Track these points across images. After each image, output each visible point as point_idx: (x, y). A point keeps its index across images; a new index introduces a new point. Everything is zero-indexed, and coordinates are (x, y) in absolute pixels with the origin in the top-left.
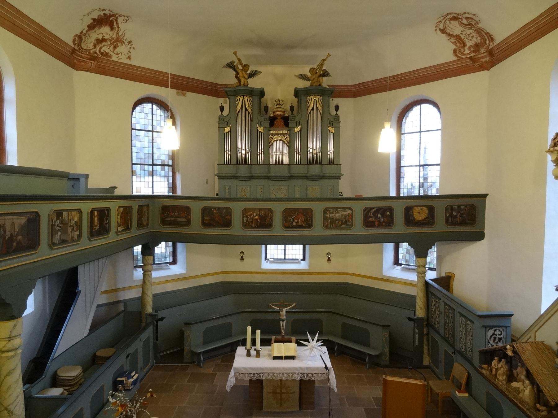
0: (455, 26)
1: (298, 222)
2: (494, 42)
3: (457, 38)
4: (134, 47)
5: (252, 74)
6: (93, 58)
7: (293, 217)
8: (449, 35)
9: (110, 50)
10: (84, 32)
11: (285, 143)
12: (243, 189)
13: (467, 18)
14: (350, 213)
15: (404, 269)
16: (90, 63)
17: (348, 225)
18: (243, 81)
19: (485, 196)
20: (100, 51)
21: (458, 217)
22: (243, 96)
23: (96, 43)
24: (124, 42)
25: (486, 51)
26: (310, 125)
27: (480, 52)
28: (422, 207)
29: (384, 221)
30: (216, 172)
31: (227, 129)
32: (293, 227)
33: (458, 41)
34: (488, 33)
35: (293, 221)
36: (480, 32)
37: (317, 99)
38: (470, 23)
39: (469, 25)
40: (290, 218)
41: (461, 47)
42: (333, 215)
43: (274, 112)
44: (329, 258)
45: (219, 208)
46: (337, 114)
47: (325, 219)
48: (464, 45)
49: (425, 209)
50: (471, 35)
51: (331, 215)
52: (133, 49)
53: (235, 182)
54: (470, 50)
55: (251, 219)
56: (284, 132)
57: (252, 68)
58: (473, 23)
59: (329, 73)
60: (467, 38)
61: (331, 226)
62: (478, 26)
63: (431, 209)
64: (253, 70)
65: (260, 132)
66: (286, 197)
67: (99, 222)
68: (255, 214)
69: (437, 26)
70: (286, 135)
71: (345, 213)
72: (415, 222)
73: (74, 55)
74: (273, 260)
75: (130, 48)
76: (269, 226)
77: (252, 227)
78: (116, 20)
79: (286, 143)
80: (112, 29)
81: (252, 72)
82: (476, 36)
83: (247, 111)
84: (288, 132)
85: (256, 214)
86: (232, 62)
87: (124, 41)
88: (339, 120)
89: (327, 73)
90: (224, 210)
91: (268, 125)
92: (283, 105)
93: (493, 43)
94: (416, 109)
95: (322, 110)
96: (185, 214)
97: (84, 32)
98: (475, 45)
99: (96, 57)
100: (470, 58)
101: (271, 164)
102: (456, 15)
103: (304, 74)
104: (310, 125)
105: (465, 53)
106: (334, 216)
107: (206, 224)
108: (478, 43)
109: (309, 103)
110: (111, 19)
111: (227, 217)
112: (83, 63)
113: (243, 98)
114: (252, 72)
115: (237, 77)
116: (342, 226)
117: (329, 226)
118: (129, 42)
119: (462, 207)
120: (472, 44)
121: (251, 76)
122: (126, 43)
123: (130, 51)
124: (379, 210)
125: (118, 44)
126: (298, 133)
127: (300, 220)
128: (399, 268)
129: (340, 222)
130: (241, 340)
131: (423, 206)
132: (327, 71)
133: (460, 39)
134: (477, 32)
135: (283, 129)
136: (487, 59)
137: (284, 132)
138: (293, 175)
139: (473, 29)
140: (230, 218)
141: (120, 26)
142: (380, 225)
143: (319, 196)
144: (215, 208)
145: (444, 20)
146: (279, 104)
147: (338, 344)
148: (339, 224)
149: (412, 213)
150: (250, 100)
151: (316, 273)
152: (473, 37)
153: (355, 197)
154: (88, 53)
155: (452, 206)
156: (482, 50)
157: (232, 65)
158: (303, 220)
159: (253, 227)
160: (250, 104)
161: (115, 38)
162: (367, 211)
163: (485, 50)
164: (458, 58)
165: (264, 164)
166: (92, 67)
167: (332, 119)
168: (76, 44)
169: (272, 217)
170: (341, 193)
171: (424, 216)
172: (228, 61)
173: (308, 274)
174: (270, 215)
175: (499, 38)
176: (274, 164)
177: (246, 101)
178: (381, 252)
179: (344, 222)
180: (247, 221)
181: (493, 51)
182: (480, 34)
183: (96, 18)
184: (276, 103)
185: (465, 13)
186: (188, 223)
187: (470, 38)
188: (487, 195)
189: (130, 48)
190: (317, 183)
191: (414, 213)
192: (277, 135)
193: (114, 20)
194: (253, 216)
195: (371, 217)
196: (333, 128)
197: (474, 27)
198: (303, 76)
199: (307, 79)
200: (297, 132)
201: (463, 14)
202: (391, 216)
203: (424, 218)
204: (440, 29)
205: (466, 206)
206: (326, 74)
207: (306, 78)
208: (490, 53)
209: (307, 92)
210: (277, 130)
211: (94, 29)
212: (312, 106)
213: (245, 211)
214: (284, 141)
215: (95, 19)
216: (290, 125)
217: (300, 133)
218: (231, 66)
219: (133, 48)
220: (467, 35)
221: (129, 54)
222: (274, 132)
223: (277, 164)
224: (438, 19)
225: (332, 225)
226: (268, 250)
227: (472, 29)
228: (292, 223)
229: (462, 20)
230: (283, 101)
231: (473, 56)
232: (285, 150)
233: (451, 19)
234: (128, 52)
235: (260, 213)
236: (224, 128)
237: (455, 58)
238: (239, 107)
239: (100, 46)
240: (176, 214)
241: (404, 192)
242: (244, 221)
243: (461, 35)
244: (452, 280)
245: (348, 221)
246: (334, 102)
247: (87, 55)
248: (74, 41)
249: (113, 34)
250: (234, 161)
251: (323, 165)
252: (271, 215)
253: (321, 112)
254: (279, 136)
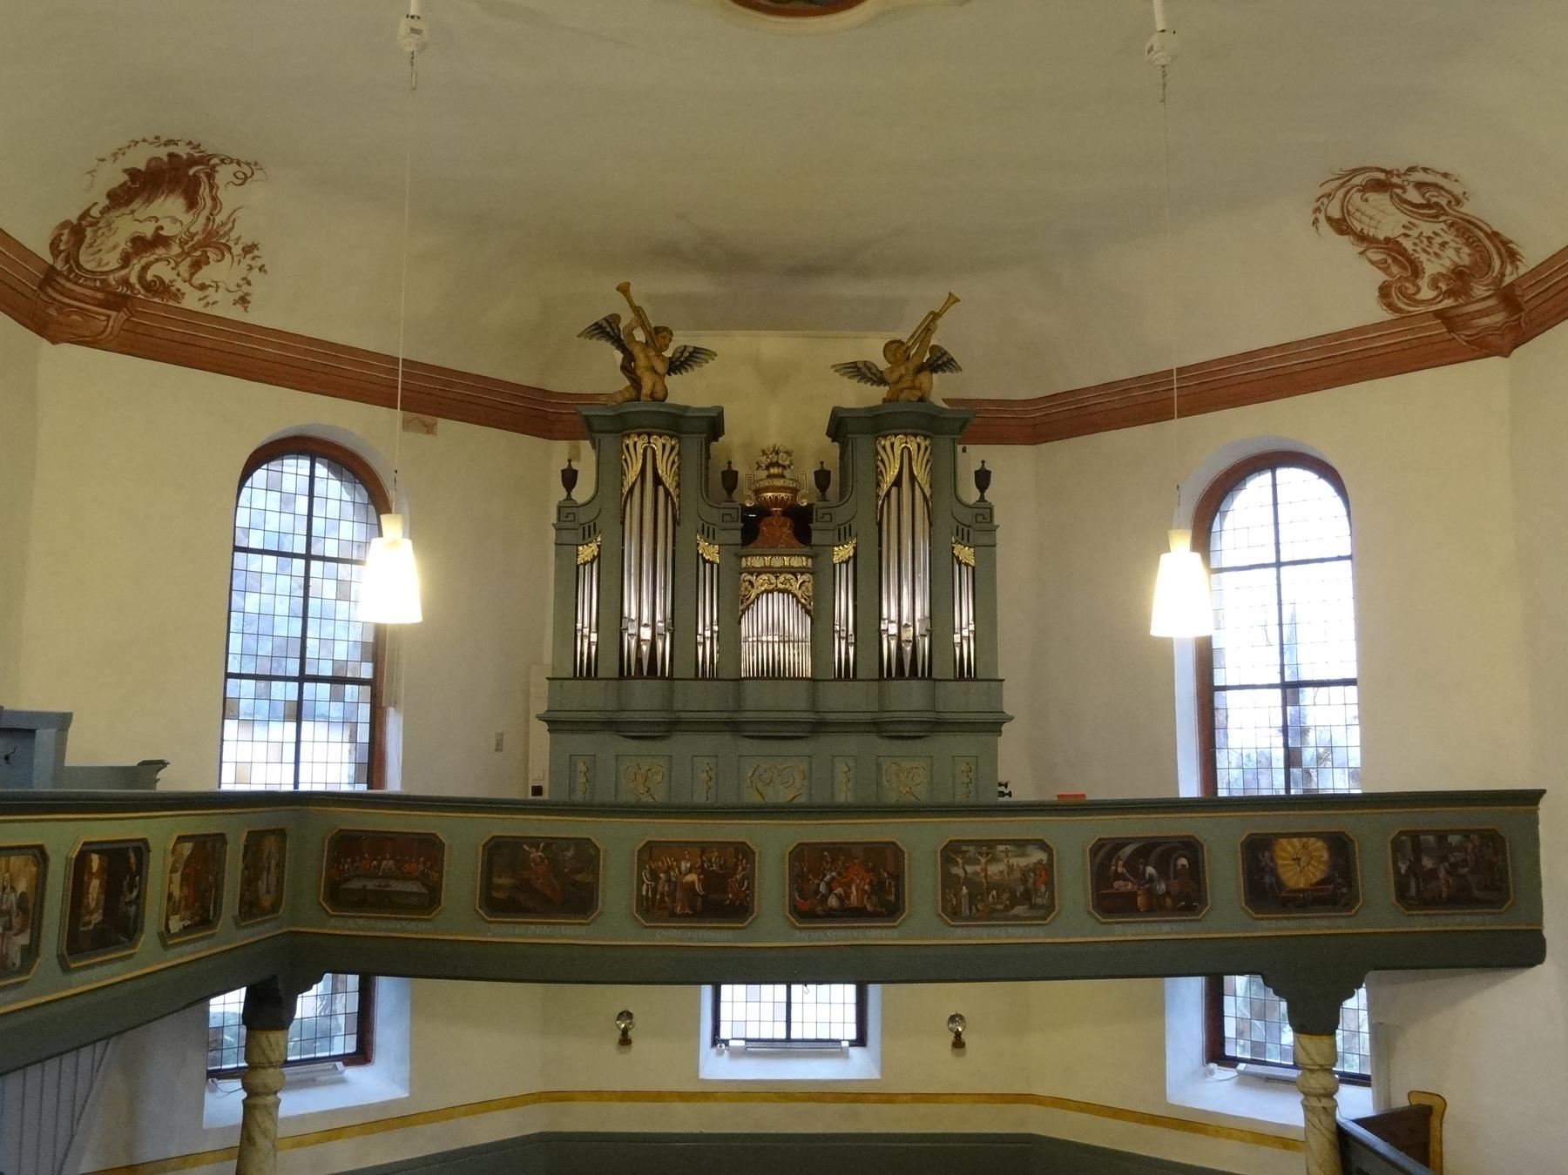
0: (1380, 208)
1: (848, 895)
2: (1518, 263)
3: (1391, 250)
4: (263, 266)
5: (682, 359)
6: (116, 300)
7: (828, 877)
8: (1362, 238)
9: (178, 275)
10: (95, 212)
11: (798, 602)
12: (643, 771)
13: (1419, 185)
14: (1040, 862)
15: (1246, 1080)
16: (104, 318)
17: (1033, 907)
18: (647, 383)
19: (1533, 797)
20: (141, 278)
21: (1442, 874)
22: (649, 435)
23: (130, 250)
24: (229, 249)
25: (1490, 293)
26: (888, 540)
27: (1474, 295)
28: (1305, 840)
29: (1168, 893)
30: (542, 708)
31: (587, 552)
32: (830, 915)
33: (1395, 260)
34: (1496, 234)
35: (830, 890)
36: (1469, 230)
37: (913, 447)
38: (1434, 200)
39: (1428, 206)
40: (816, 881)
41: (1406, 279)
42: (978, 868)
43: (758, 492)
44: (958, 1035)
45: (550, 843)
46: (982, 499)
47: (949, 882)
48: (1416, 271)
49: (1317, 845)
50: (1438, 240)
51: (969, 869)
52: (260, 269)
53: (609, 746)
54: (1437, 287)
55: (669, 886)
56: (797, 562)
57: (681, 340)
58: (1444, 202)
59: (952, 359)
60: (1424, 251)
61: (971, 909)
62: (1460, 212)
63: (1340, 845)
64: (685, 347)
65: (708, 561)
66: (803, 799)
67: (102, 897)
68: (685, 865)
69: (1317, 210)
70: (802, 574)
71: (1022, 862)
72: (1283, 894)
73: (50, 291)
74: (742, 1043)
75: (251, 268)
76: (888, 907)
77: (673, 915)
78: (210, 176)
79: (803, 601)
80: (192, 204)
81: (682, 353)
82: (1457, 243)
83: (661, 489)
84: (810, 560)
85: (689, 865)
86: (613, 320)
87: (231, 244)
88: (991, 521)
89: (945, 359)
90: (567, 850)
91: (737, 537)
92: (789, 466)
93: (1517, 268)
94: (1258, 485)
95: (931, 486)
96: (421, 867)
97: (95, 212)
98: (1453, 271)
99: (126, 297)
100: (1439, 314)
101: (746, 678)
102: (1382, 176)
103: (865, 363)
104: (888, 540)
105: (1420, 296)
106: (982, 874)
107: (496, 905)
108: (1464, 266)
109: (882, 461)
110: (191, 172)
111: (579, 877)
112: (78, 318)
113: (649, 443)
114: (682, 353)
115: (628, 368)
116: (1012, 912)
117: (965, 911)
118: (249, 246)
119: (1454, 839)
120: (1444, 271)
121: (677, 365)
122: (237, 250)
123: (249, 278)
124: (1148, 848)
125: (209, 254)
126: (844, 566)
127: (854, 889)
128: (1230, 1073)
129: (1005, 896)
131: (1309, 835)
132: (946, 353)
133: (1403, 252)
134: (1458, 230)
135: (788, 551)
136: (1498, 318)
137: (797, 562)
138: (830, 717)
139: (1445, 221)
140: (590, 878)
141: (221, 194)
142: (1155, 907)
143: (923, 795)
144: (534, 842)
145: (1343, 191)
146: (776, 464)
148: (1001, 903)
149: (1272, 860)
150: (673, 448)
151: (910, 1097)
152: (1443, 245)
153: (1056, 799)
154: (98, 284)
155: (1415, 836)
156: (1480, 290)
157: (613, 329)
158: (866, 887)
159: (679, 916)
160: (673, 462)
161: (200, 233)
162: (1104, 853)
163: (1487, 290)
164: (1398, 315)
165: (720, 676)
166: (109, 329)
167: (967, 517)
168: (61, 252)
169: (750, 877)
170: (1006, 786)
171: (1316, 872)
172: (599, 317)
173: (875, 1102)
174: (740, 868)
175: (1533, 254)
176: (758, 678)
177: (659, 453)
178: (1157, 1011)
179: (1018, 894)
180: (655, 891)
181: (1518, 292)
182: (1470, 237)
183: (142, 166)
184: (764, 461)
185: (1412, 169)
186: (430, 901)
187: (1436, 248)
188: (1541, 793)
189: (251, 268)
190: (918, 746)
191: (1280, 862)
192: (766, 573)
193: (202, 175)
194: (680, 872)
195: (1119, 877)
196: (972, 550)
197: (1446, 214)
198: (860, 369)
199: (879, 379)
200: (843, 562)
201: (1407, 170)
202: (1196, 870)
203: (1315, 881)
204: (1329, 219)
205: (1467, 837)
206: (941, 362)
207: (871, 373)
208: (1508, 298)
209: (877, 423)
210: (767, 555)
211: (128, 202)
212: (896, 471)
213: (650, 851)
214: (794, 596)
215: (139, 171)
216: (816, 537)
217: (851, 562)
218: (609, 333)
219: (261, 269)
220: (1425, 240)
221: (246, 288)
222: (757, 562)
223: (768, 678)
224: (1321, 186)
225: (973, 907)
226: (722, 1004)
227: (1440, 220)
228: (825, 898)
229: (1405, 191)
230: (788, 453)
231: (1452, 307)
232: (799, 626)
233: (1364, 189)
234: (241, 282)
235: (703, 862)
236: (577, 545)
237: (1387, 316)
238: (632, 475)
239: (144, 261)
240: (388, 864)
241: (1230, 783)
242: (644, 893)
243: (1401, 240)
244: (1434, 1121)
245: (1036, 890)
246: (973, 457)
247: (96, 289)
248: (54, 246)
249: (193, 222)
250: (609, 667)
251: (936, 680)
252: (744, 869)
253: (928, 494)
254: (777, 577)
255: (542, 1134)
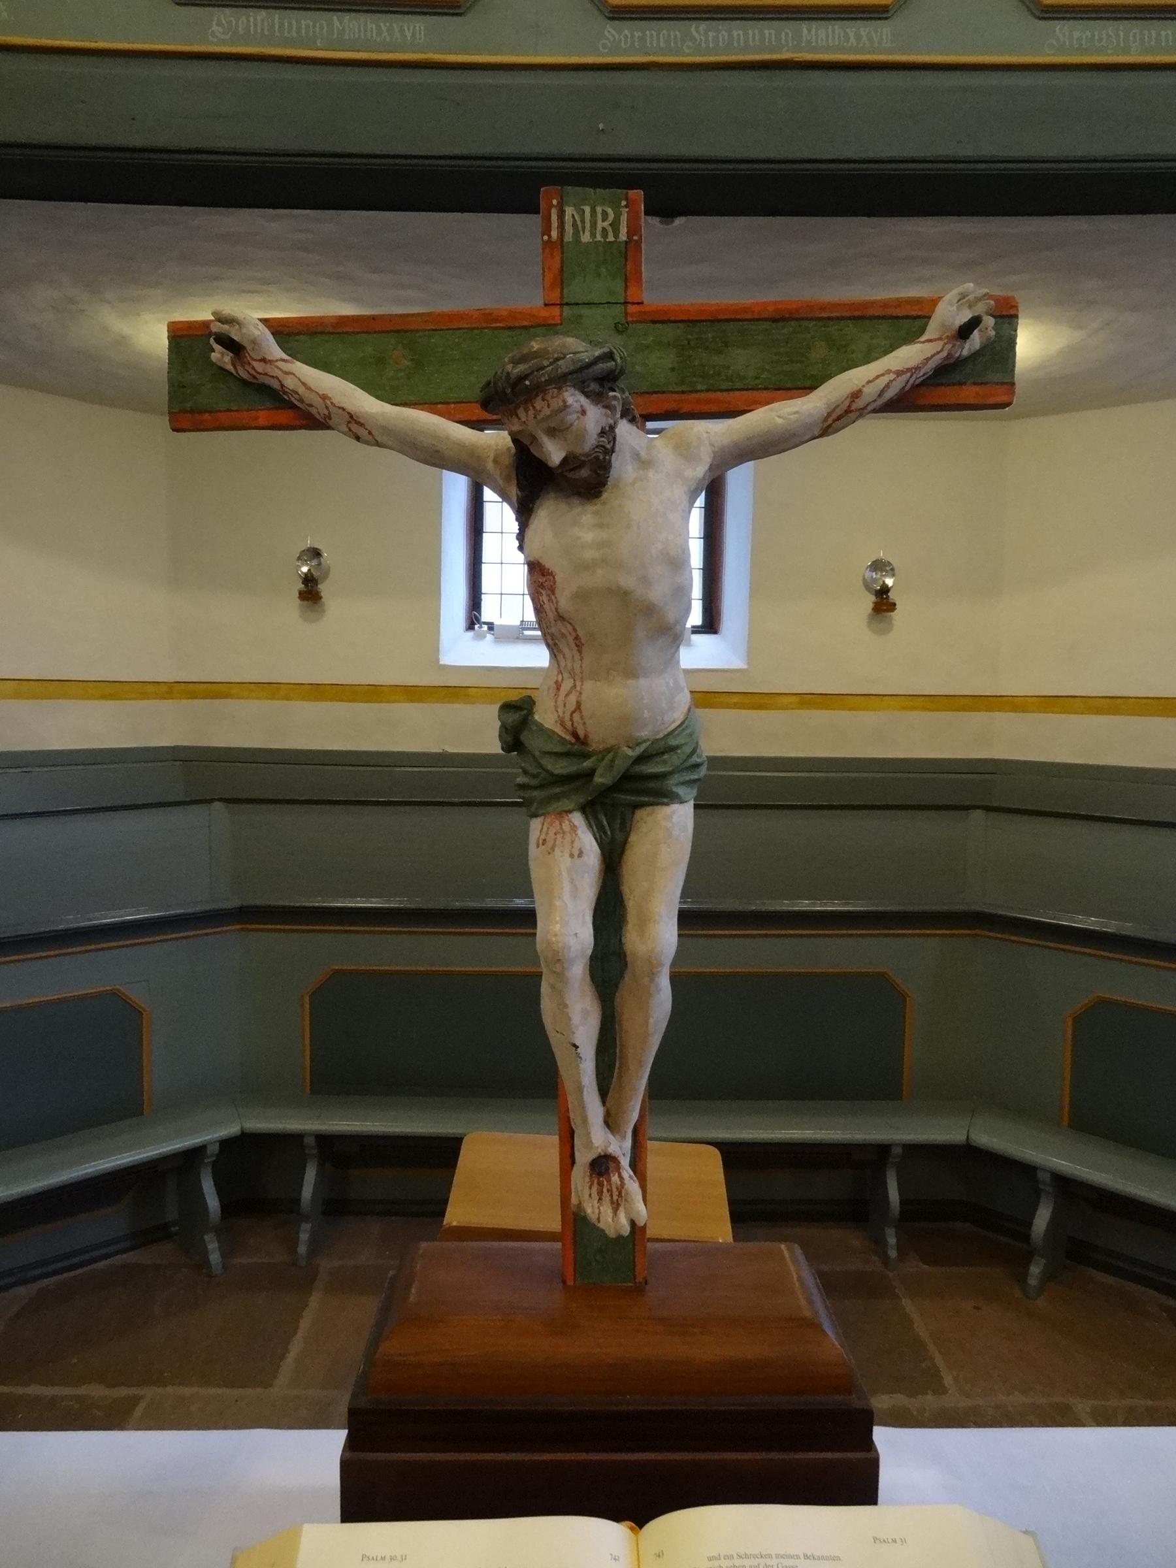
130: (214, 1149)
147: (1065, 1185)
151: (793, 699)
173: (736, 706)
226: (484, 566)
255: (174, 749)
